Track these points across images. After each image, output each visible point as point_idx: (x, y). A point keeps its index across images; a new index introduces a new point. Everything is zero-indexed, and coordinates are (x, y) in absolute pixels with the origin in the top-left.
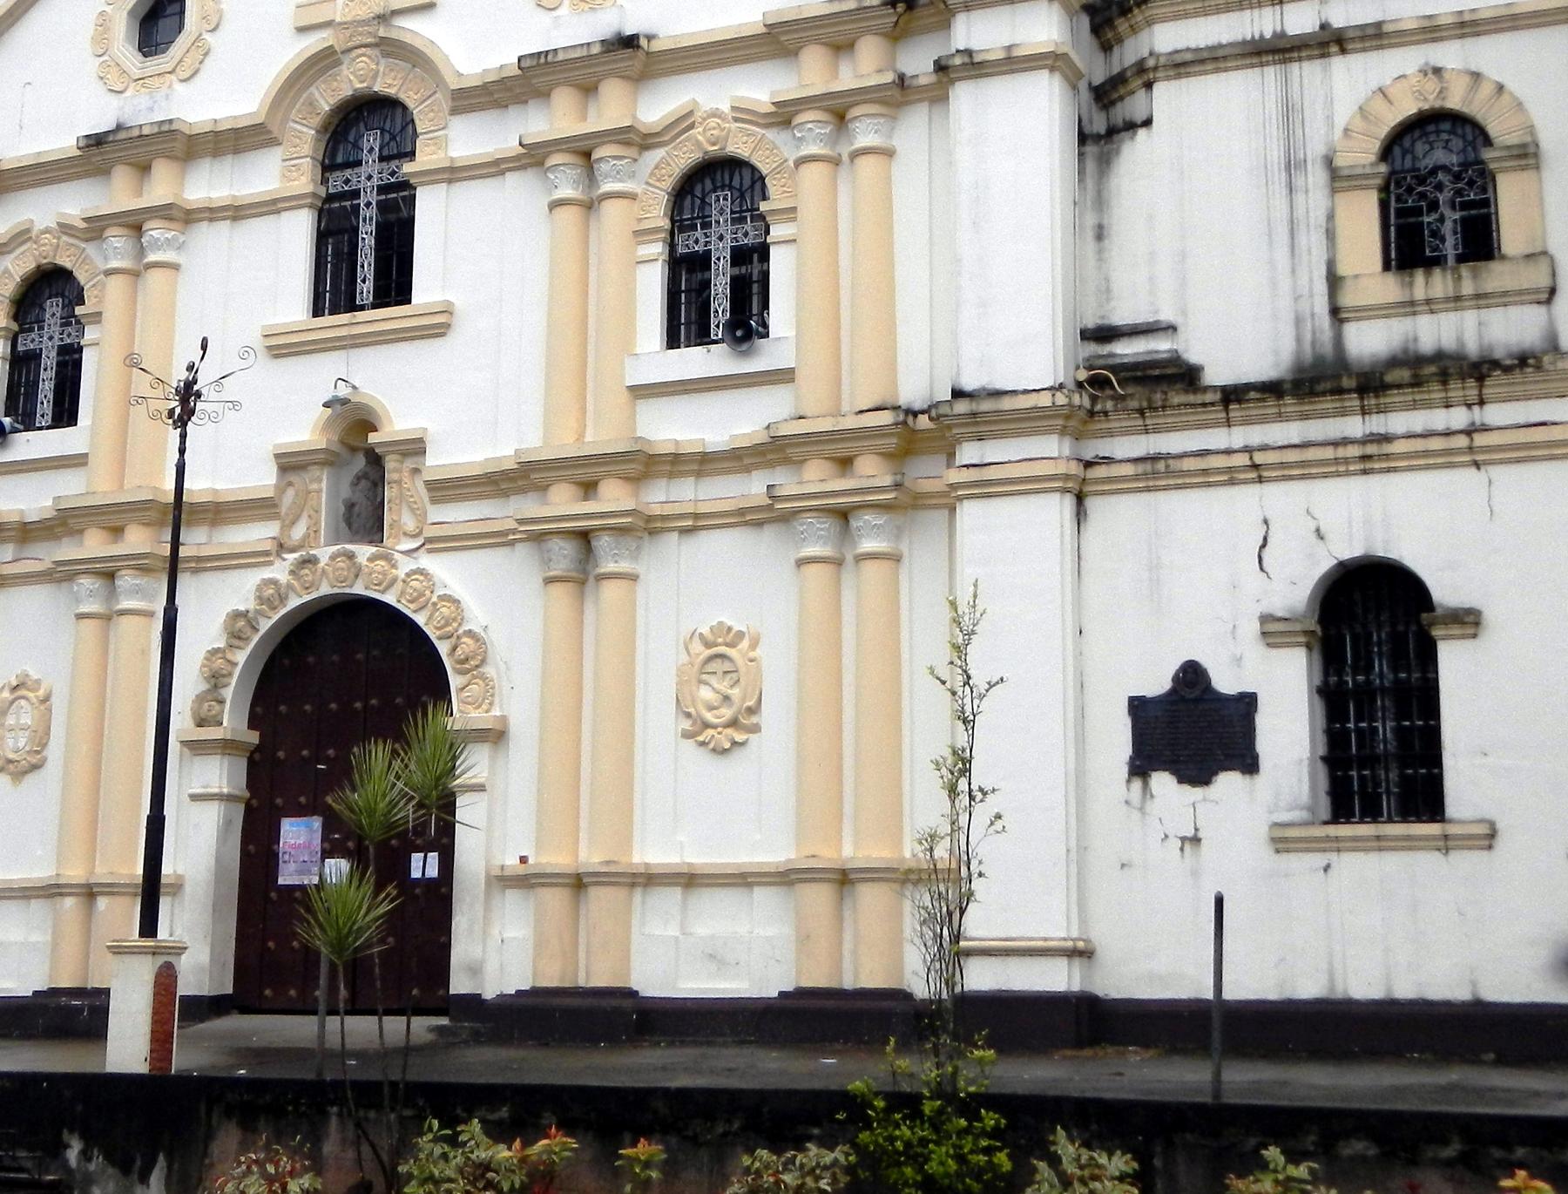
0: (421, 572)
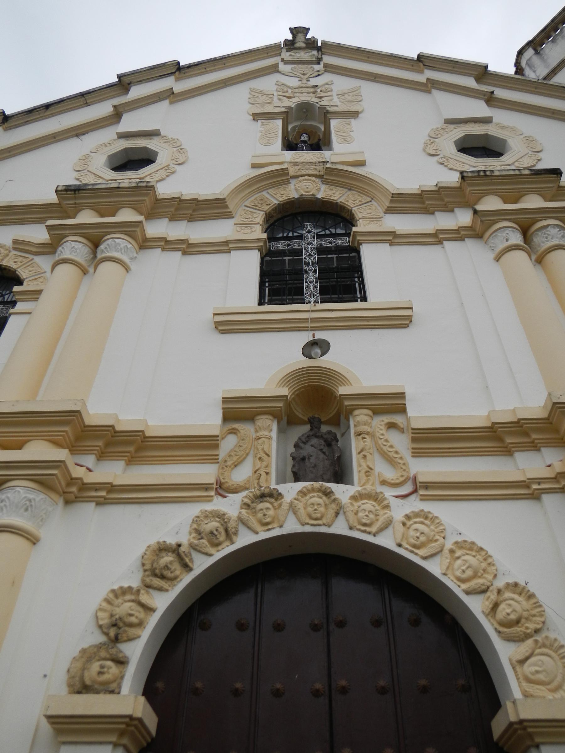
0: (426, 516)
